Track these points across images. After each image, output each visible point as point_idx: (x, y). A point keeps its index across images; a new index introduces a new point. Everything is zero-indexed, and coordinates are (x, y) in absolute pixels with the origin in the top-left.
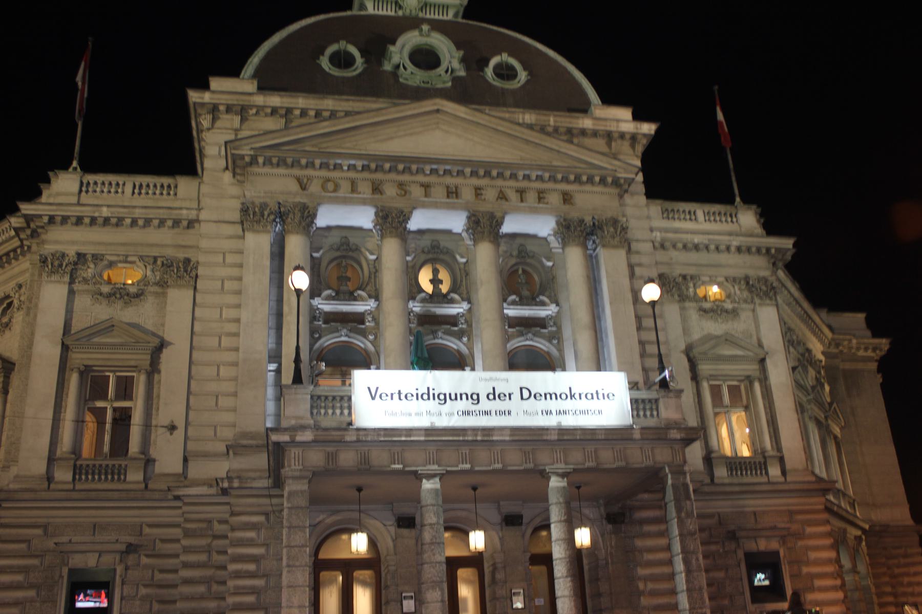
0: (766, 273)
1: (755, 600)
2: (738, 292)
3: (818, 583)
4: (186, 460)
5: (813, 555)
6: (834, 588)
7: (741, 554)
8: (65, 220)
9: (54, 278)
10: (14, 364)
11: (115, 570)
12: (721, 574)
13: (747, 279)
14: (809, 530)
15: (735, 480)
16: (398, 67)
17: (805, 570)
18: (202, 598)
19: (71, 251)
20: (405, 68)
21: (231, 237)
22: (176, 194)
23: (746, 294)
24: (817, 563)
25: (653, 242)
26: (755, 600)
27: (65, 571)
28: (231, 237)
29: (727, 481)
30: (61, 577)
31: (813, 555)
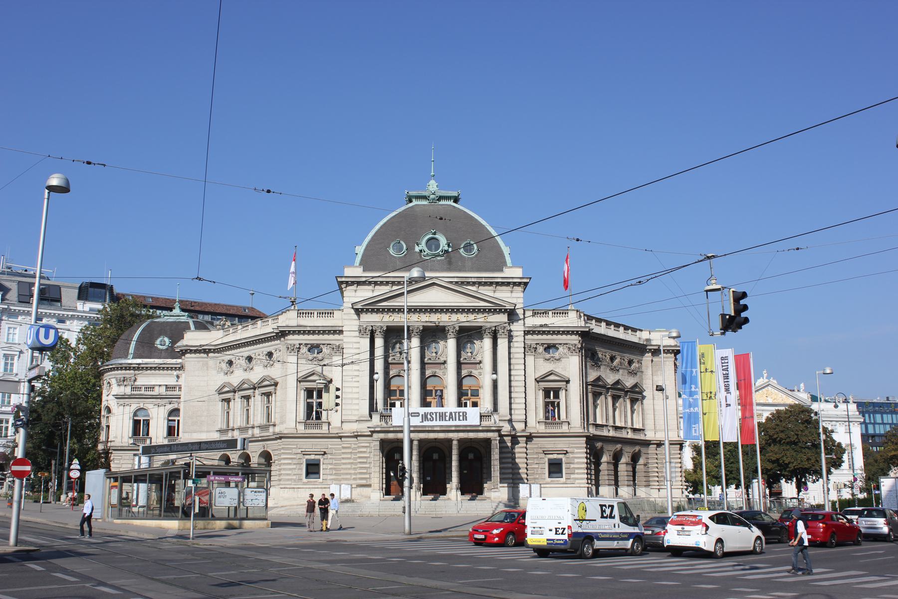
0: (577, 342)
1: (549, 477)
2: (562, 350)
3: (577, 471)
4: (342, 422)
5: (576, 460)
6: (583, 473)
7: (546, 460)
8: (294, 331)
9: (292, 354)
10: (278, 383)
11: (320, 460)
12: (536, 466)
13: (567, 344)
14: (576, 451)
15: (548, 431)
16: (421, 251)
17: (572, 466)
18: (349, 469)
19: (297, 342)
20: (424, 252)
21: (355, 337)
22: (333, 317)
23: (566, 350)
24: (578, 463)
25: (524, 331)
26: (549, 477)
27: (304, 460)
28: (355, 337)
29: (544, 431)
30: (303, 462)
31: (576, 460)
